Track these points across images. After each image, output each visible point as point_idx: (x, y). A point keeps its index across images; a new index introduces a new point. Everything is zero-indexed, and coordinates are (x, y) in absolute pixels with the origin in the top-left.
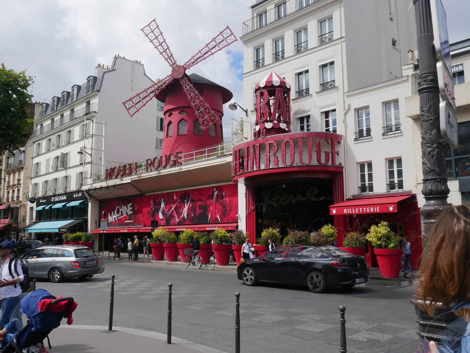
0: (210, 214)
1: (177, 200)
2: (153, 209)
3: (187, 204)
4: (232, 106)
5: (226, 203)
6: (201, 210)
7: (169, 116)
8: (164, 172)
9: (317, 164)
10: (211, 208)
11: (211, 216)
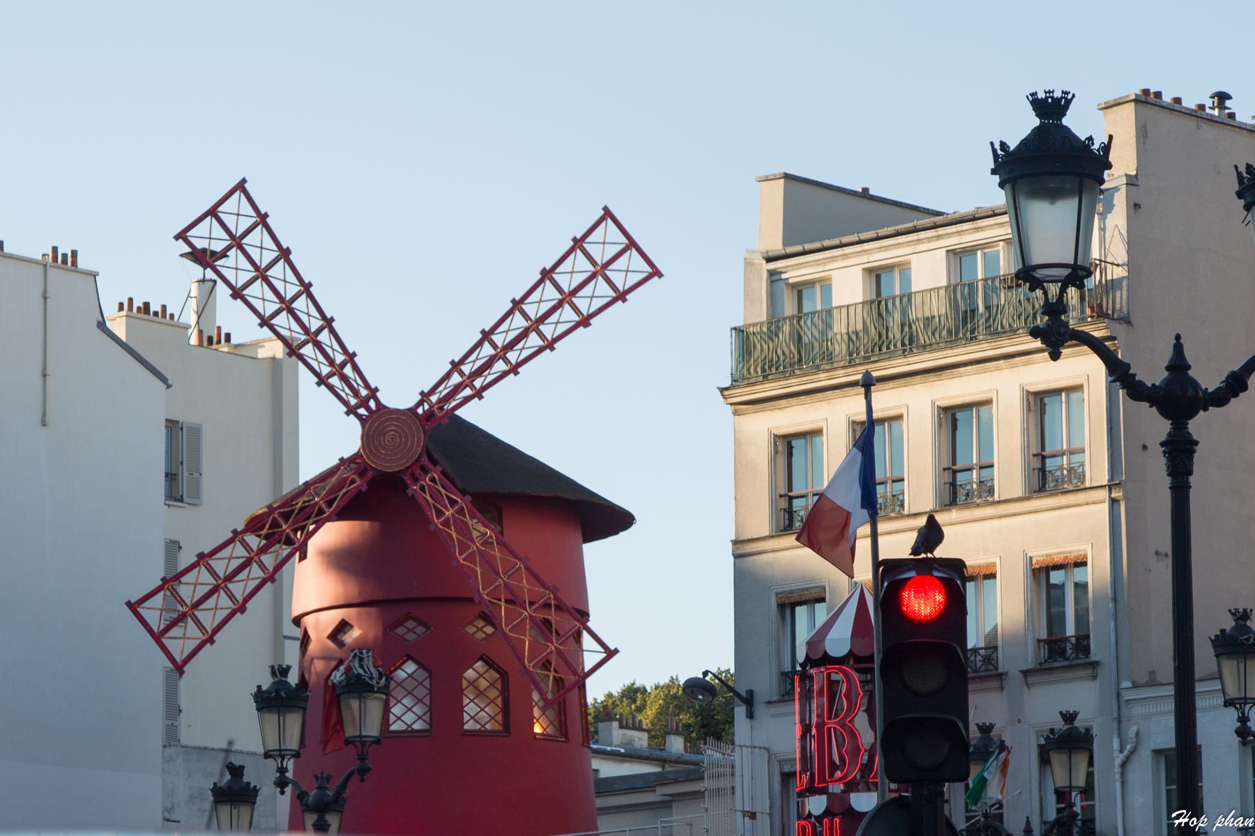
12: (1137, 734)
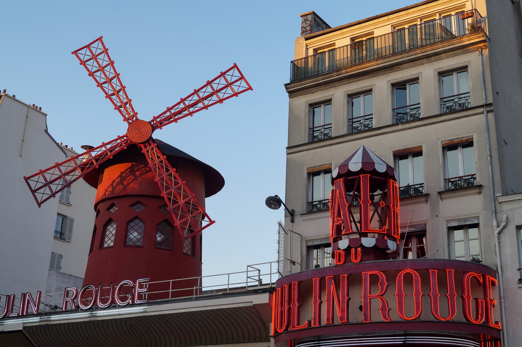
4: (272, 201)
7: (109, 209)
8: (104, 314)
9: (463, 320)
12: (507, 218)
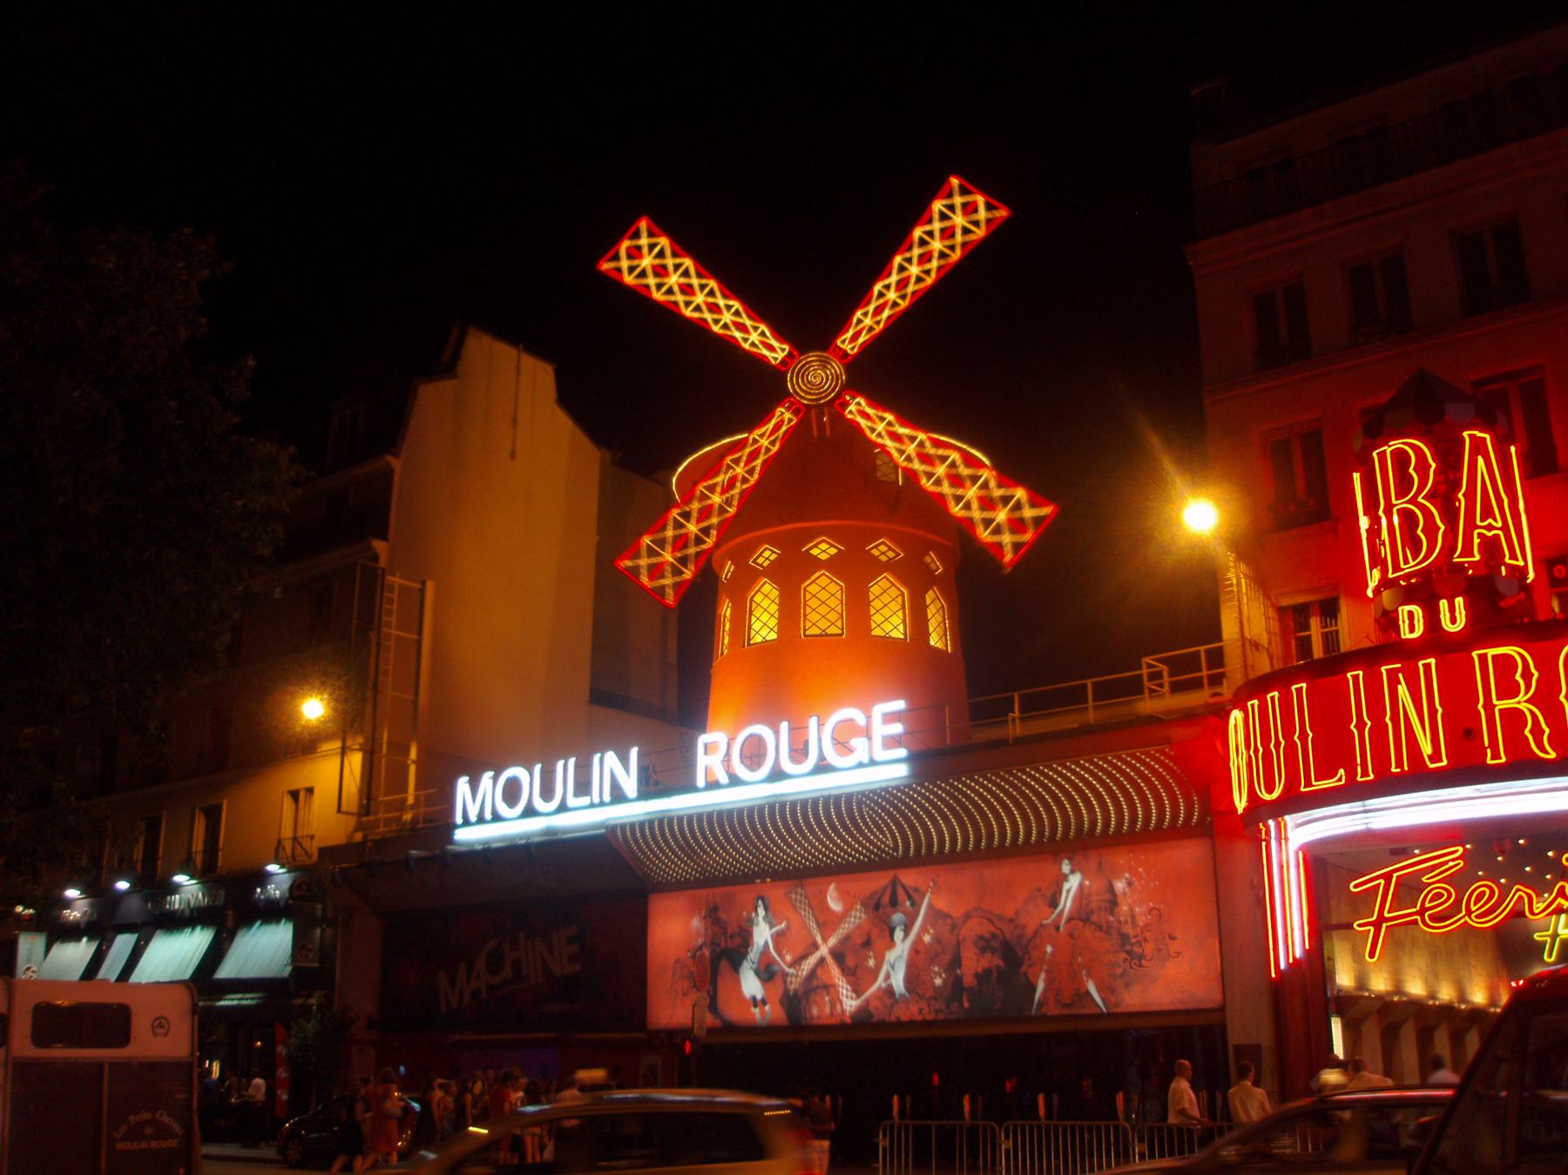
0: (1042, 976)
1: (845, 914)
2: (707, 952)
3: (907, 932)
5: (1134, 923)
6: (988, 956)
10: (1049, 949)
11: (1048, 982)
